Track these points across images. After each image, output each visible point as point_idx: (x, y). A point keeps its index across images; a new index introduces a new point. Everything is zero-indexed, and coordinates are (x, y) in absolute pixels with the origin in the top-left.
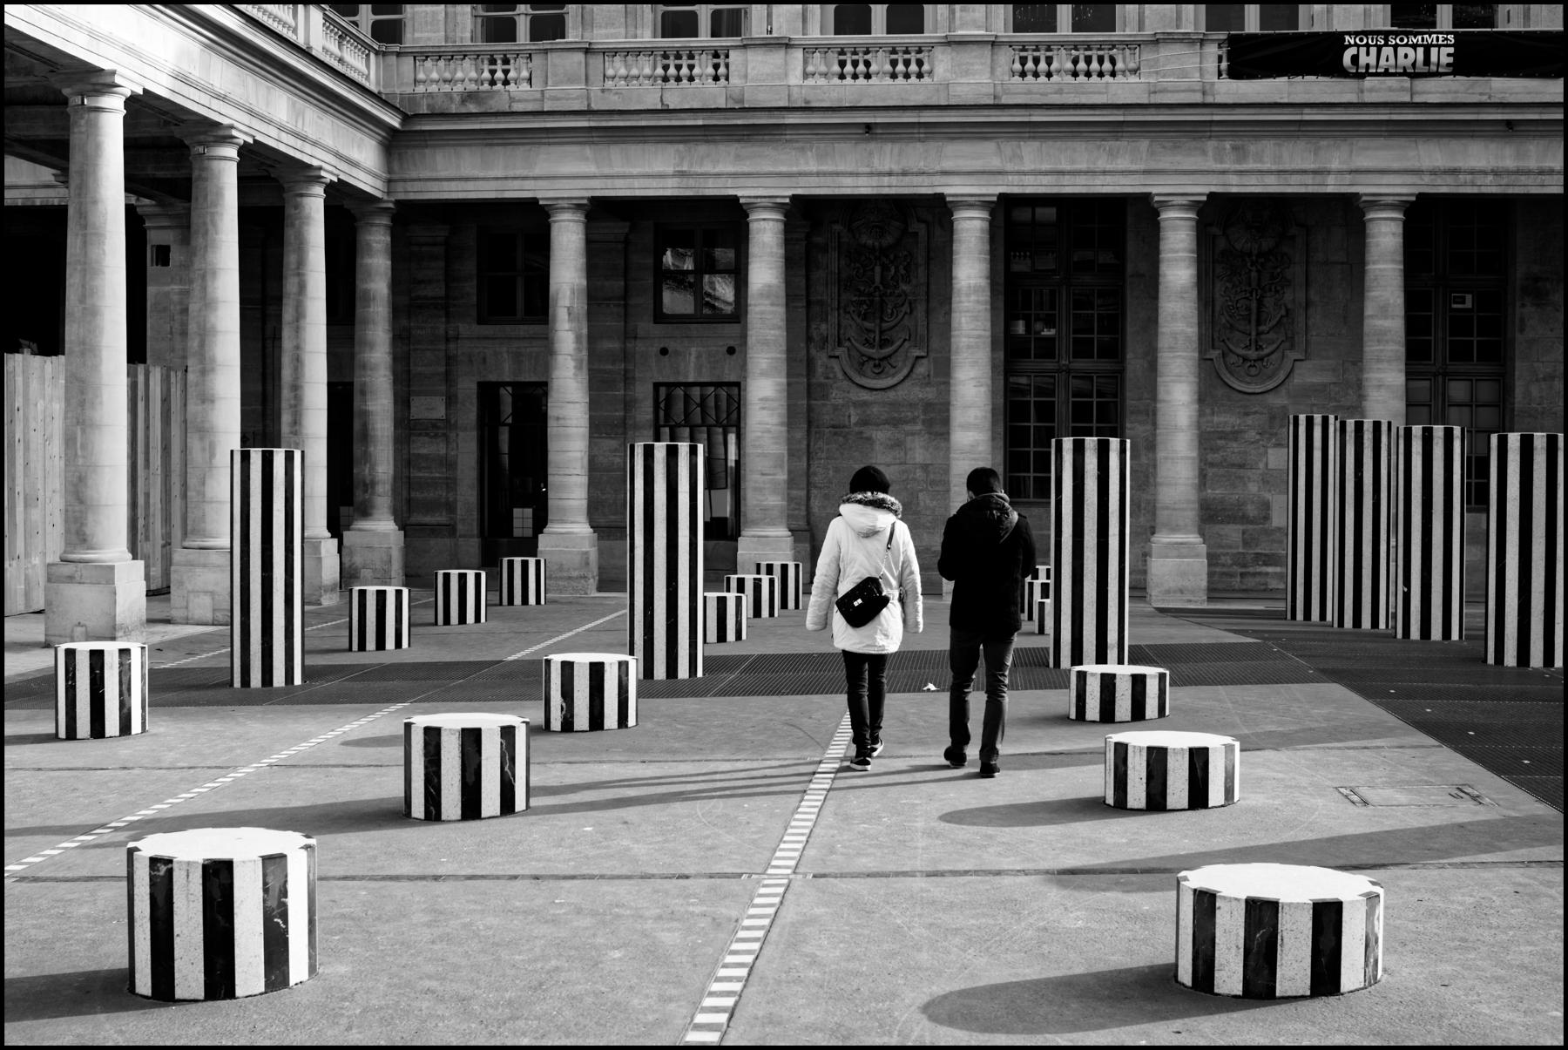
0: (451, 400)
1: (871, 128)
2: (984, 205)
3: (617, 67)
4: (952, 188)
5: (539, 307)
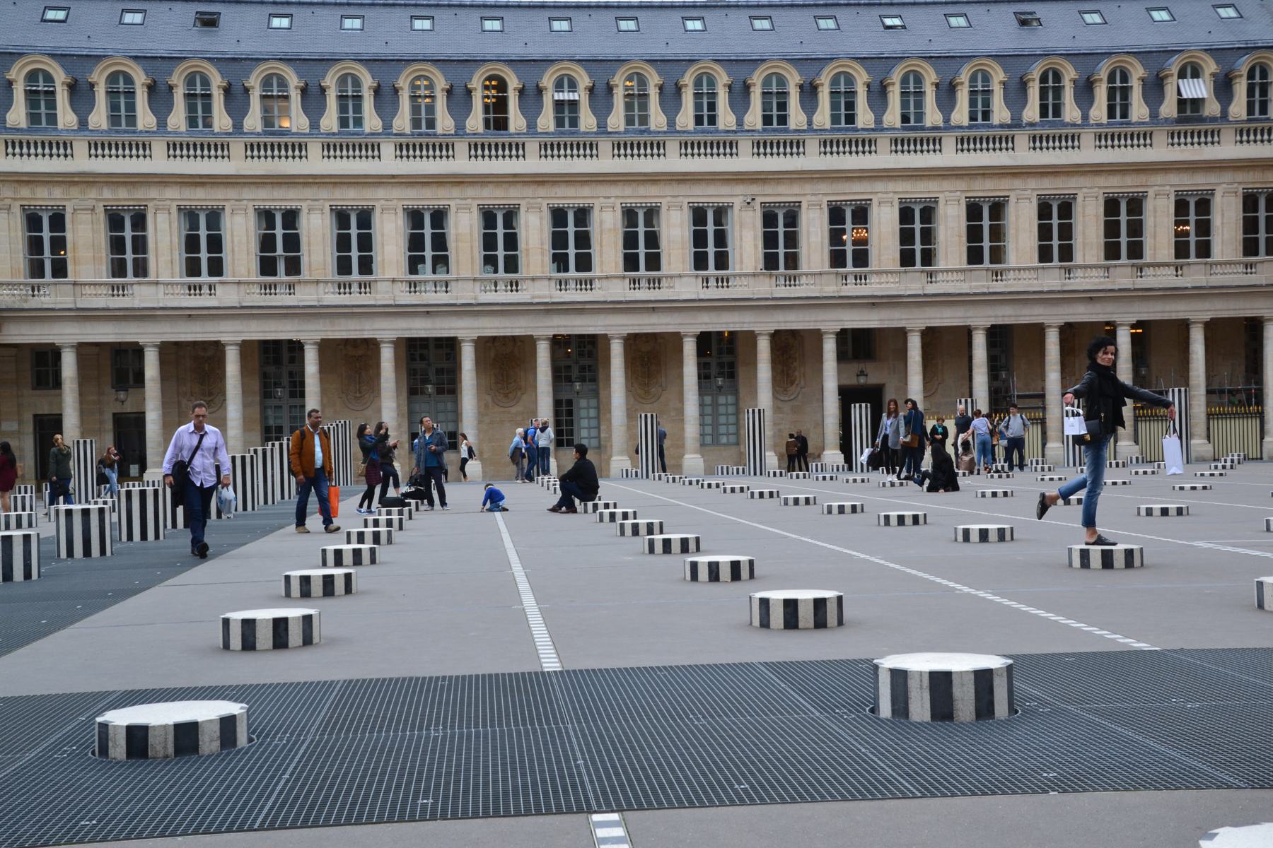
0: (20, 422)
1: (191, 315)
2: (236, 344)
3: (87, 290)
4: (223, 338)
5: (58, 384)
